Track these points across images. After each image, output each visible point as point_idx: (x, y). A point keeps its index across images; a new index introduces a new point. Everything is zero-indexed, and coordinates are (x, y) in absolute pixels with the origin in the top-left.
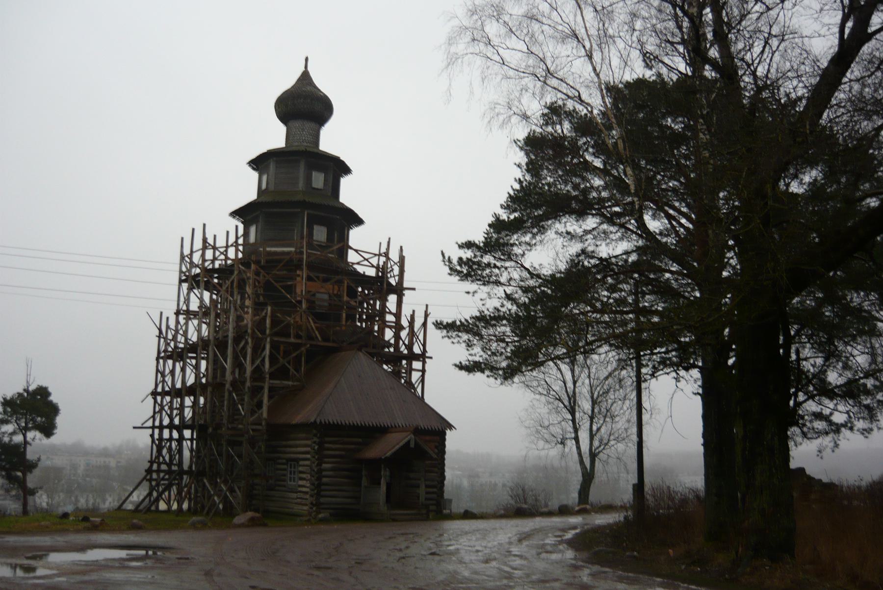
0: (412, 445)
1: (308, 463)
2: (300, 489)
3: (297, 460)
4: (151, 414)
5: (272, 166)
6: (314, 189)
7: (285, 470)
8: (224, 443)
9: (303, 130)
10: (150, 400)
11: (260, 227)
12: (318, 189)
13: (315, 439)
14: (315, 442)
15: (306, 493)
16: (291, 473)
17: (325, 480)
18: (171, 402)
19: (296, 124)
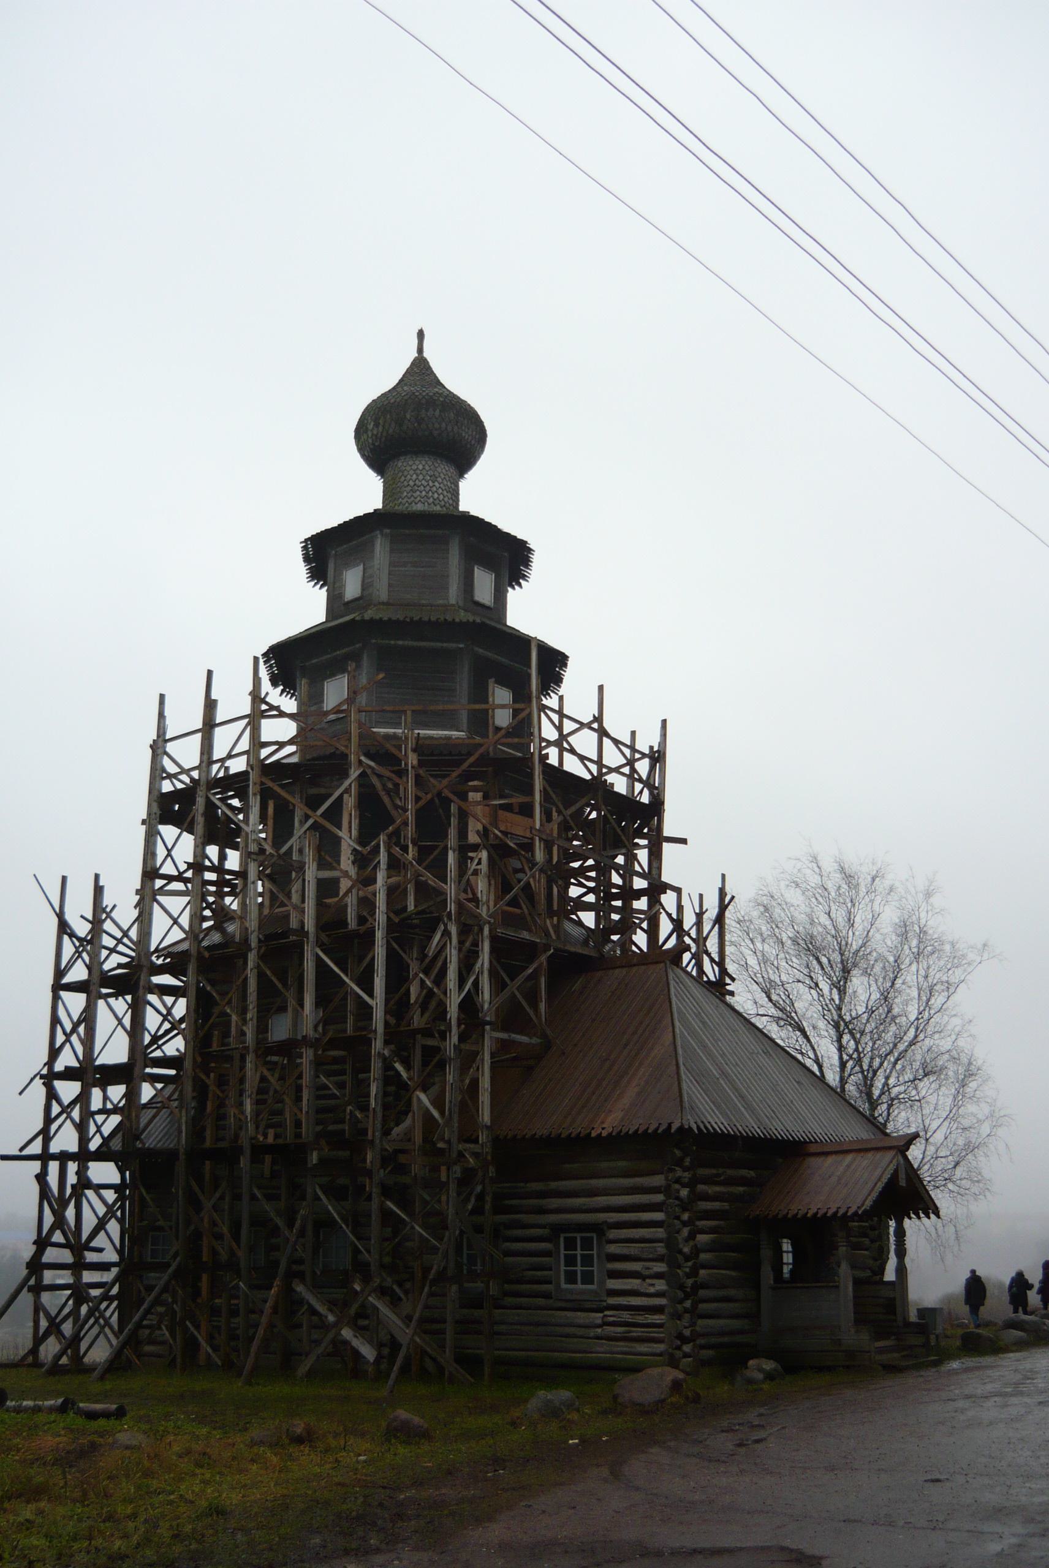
2: (612, 1301)
3: (599, 1229)
4: (40, 1125)
6: (478, 604)
7: (547, 1254)
8: (376, 1191)
9: (434, 478)
10: (38, 1090)
12: (483, 606)
13: (679, 1172)
15: (659, 1310)
16: (570, 1261)
18: (83, 1098)
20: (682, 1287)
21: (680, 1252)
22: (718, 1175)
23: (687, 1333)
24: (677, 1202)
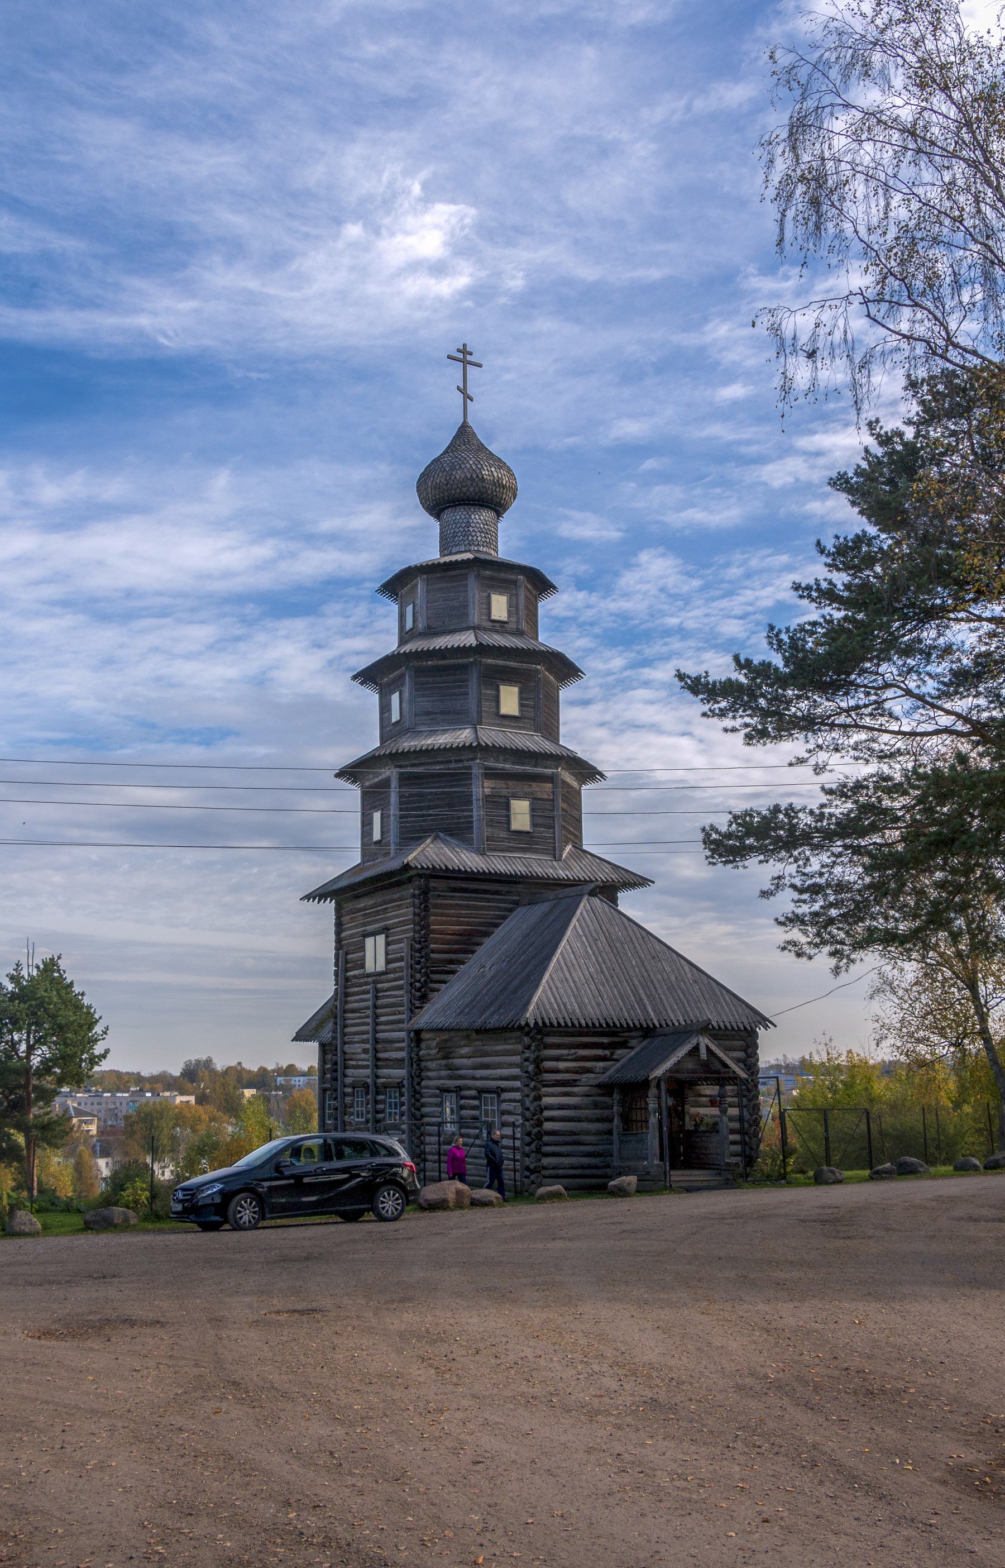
0: (703, 1055)
1: (517, 1095)
3: (499, 1091)
5: (420, 585)
11: (406, 694)
14: (527, 1060)
17: (548, 1126)
19: (457, 515)
20: (529, 1134)
21: (528, 1109)
22: (569, 1055)
23: (532, 1167)
24: (526, 1075)
